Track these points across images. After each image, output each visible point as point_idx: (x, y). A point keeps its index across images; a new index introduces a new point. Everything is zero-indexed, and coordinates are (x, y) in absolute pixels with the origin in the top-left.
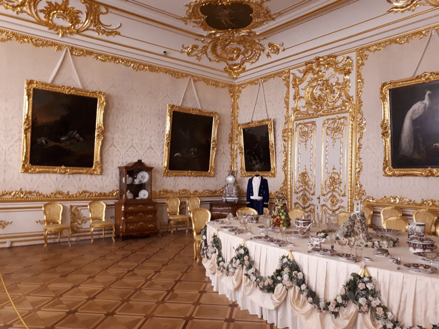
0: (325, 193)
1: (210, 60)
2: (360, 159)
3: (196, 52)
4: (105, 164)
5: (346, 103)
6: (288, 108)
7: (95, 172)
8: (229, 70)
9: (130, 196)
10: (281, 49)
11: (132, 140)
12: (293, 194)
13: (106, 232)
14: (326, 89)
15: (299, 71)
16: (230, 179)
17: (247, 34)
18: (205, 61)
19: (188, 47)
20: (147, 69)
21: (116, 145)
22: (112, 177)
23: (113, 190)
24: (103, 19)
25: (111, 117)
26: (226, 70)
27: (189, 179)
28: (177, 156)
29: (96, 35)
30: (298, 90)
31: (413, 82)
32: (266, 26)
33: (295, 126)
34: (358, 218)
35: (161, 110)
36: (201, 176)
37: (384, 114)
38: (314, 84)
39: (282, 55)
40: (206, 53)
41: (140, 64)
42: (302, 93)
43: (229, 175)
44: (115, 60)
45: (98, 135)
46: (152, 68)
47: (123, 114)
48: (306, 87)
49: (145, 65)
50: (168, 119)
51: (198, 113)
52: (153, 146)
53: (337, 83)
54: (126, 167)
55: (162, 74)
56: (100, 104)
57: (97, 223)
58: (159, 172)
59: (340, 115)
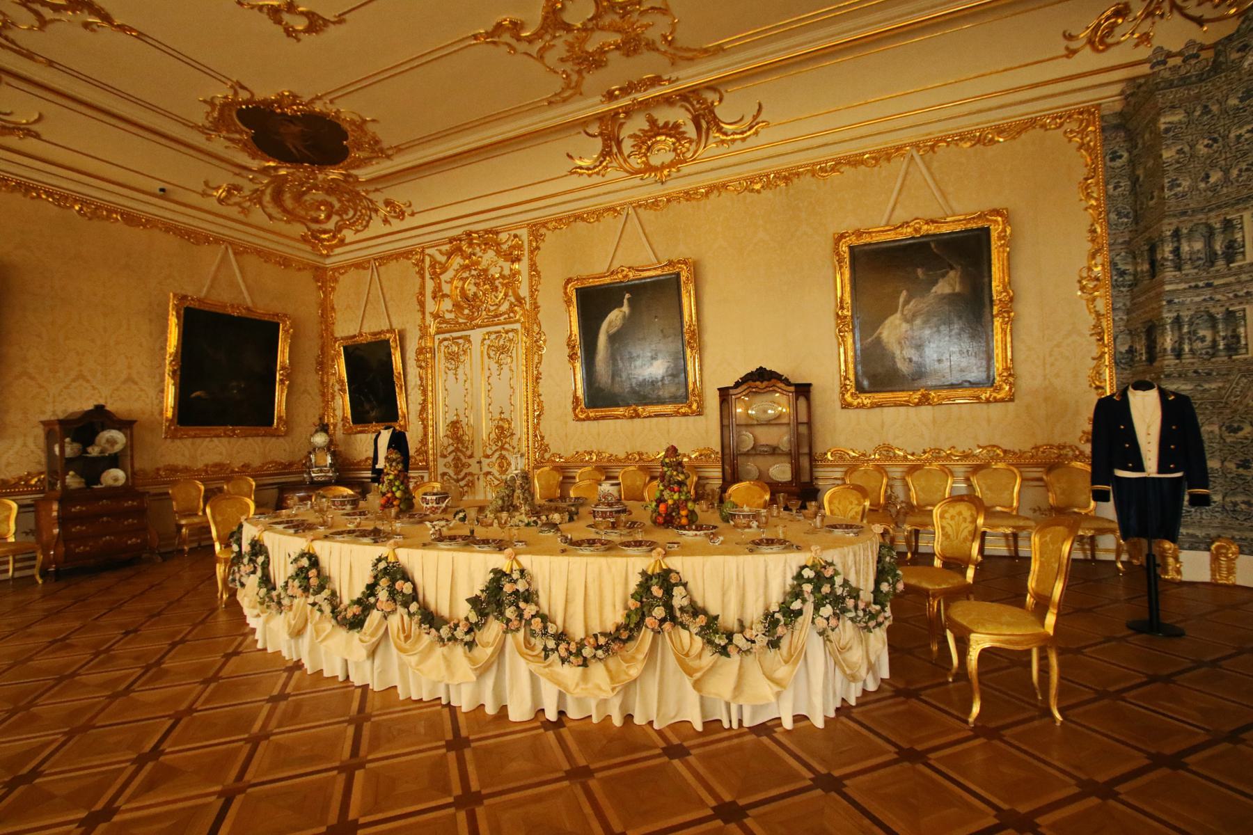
0: (489, 452)
1: (271, 217)
2: (539, 395)
6: (424, 313)
8: (313, 239)
9: (73, 480)
10: (408, 211)
11: (80, 364)
16: (320, 439)
17: (341, 178)
18: (258, 216)
19: (219, 188)
22: (25, 445)
23: (29, 474)
26: (304, 239)
28: (198, 397)
30: (440, 284)
33: (437, 342)
34: (518, 482)
36: (258, 435)
38: (466, 275)
39: (409, 222)
40: (261, 203)
41: (98, 207)
42: (446, 289)
43: (317, 431)
49: (110, 211)
50: (173, 321)
52: (135, 376)
54: (61, 422)
59: (508, 327)
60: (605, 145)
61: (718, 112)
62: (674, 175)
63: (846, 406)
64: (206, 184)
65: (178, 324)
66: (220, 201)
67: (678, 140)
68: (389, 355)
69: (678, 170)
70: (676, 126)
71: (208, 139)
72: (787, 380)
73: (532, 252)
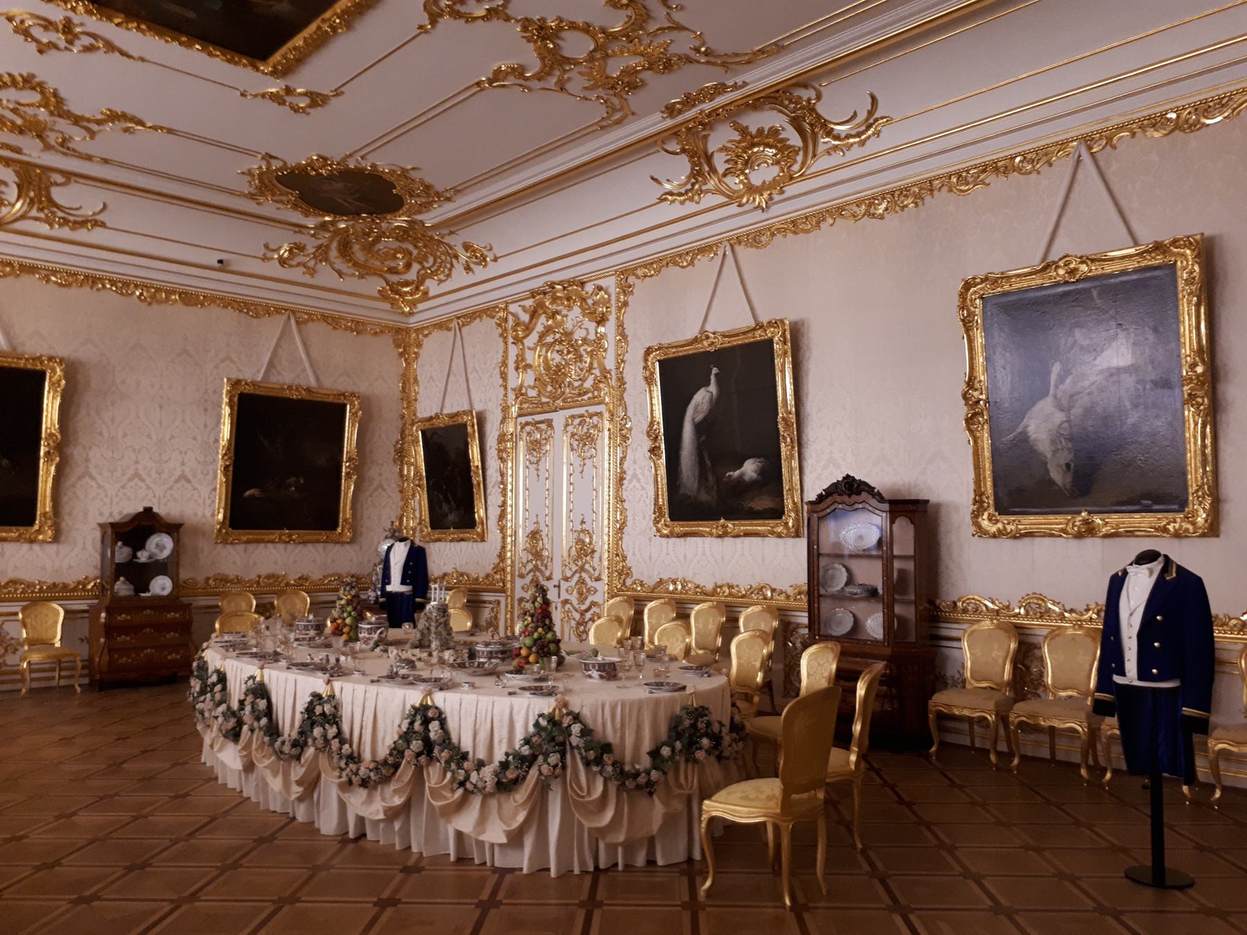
0: (569, 574)
1: (340, 274)
3: (300, 259)
4: (66, 518)
5: (601, 385)
6: (506, 388)
7: (41, 537)
9: (122, 588)
11: (137, 462)
12: (517, 579)
13: (63, 673)
14: (569, 352)
15: (523, 307)
18: (326, 276)
19: (280, 248)
20: (176, 300)
21: (95, 474)
22: (84, 548)
24: (58, 194)
25: (83, 411)
26: (383, 296)
27: (286, 550)
28: (253, 496)
29: (44, 228)
31: (690, 350)
32: (441, 210)
35: (210, 391)
36: (318, 541)
37: (652, 410)
38: (549, 339)
39: (493, 269)
41: (158, 290)
42: (530, 357)
44: (94, 282)
45: (48, 454)
46: (189, 298)
47: (113, 403)
48: (536, 345)
49: (170, 292)
50: (226, 411)
51: (305, 395)
52: (189, 475)
53: (585, 340)
54: (113, 525)
55: (216, 311)
56: (52, 384)
57: (38, 651)
58: (204, 534)
59: (592, 409)
60: (694, 164)
61: (821, 109)
62: (777, 198)
63: (981, 532)
64: (266, 246)
65: (231, 415)
66: (282, 262)
67: (780, 150)
68: (467, 444)
69: (782, 192)
70: (774, 132)
71: (259, 204)
72: (879, 494)
73: (619, 309)
